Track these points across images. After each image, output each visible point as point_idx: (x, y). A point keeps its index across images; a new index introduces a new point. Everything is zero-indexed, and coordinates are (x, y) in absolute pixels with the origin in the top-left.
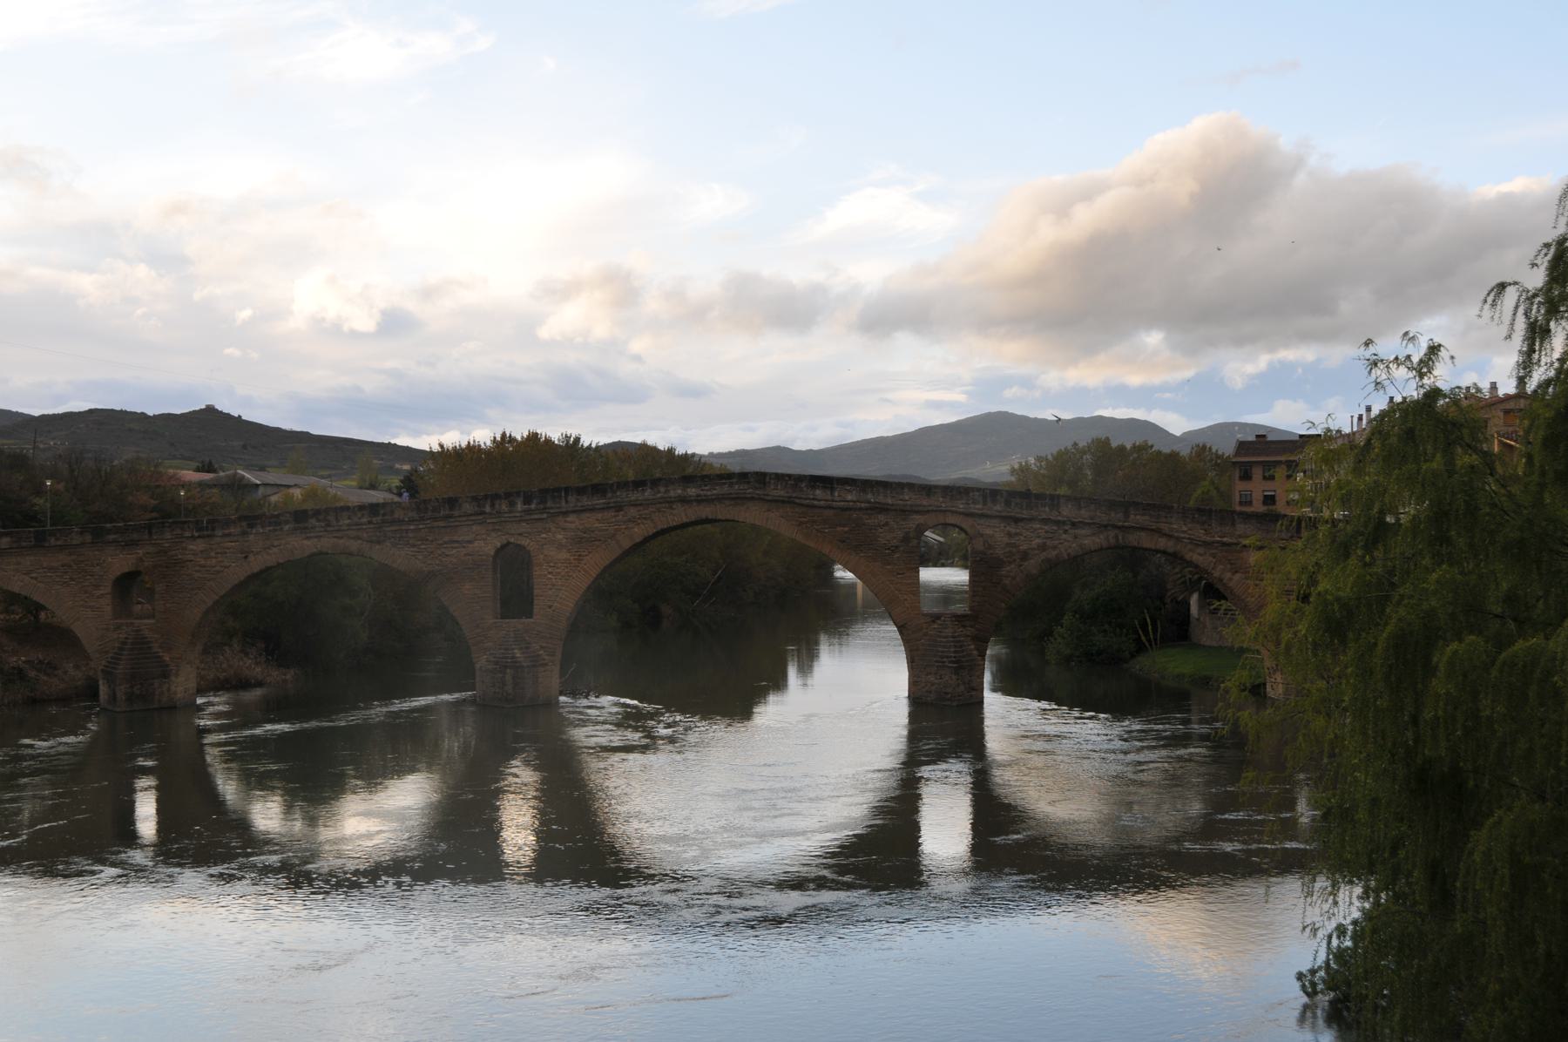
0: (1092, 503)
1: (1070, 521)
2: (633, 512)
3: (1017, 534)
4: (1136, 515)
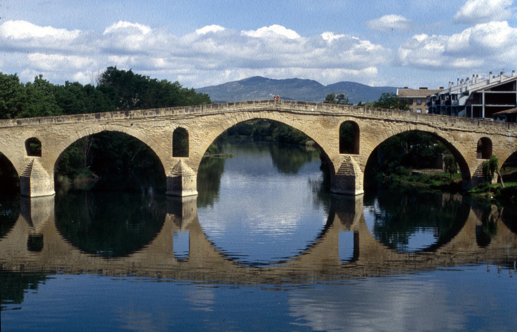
2: (228, 115)
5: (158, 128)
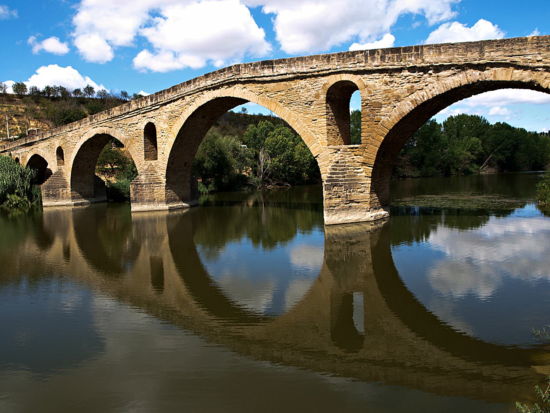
0: (450, 48)
1: (432, 66)
2: (188, 98)
3: (391, 82)
4: (490, 52)
5: (133, 125)
